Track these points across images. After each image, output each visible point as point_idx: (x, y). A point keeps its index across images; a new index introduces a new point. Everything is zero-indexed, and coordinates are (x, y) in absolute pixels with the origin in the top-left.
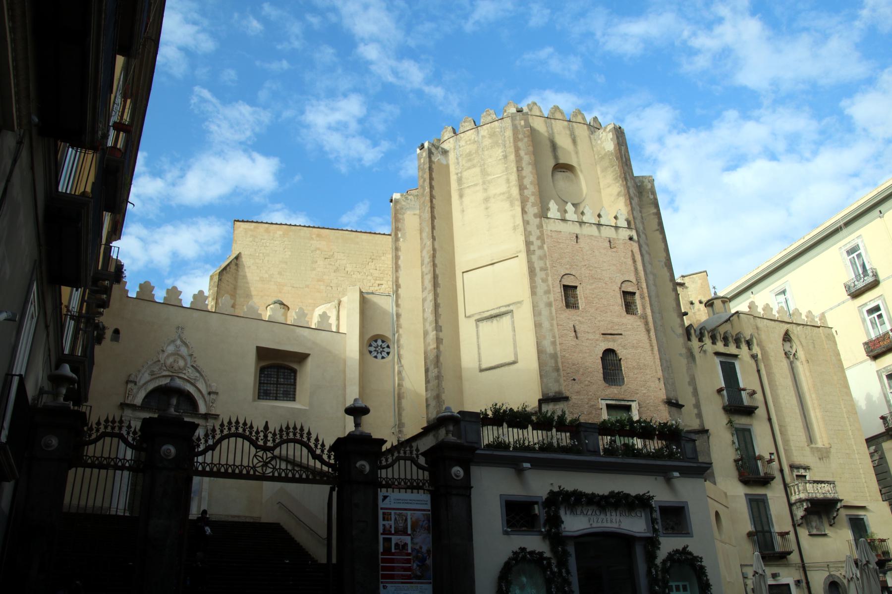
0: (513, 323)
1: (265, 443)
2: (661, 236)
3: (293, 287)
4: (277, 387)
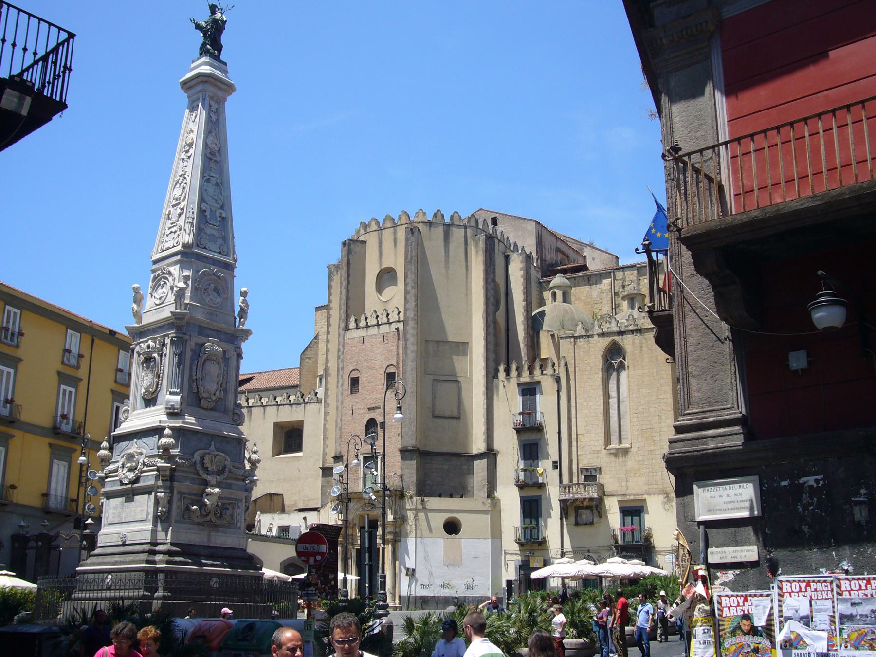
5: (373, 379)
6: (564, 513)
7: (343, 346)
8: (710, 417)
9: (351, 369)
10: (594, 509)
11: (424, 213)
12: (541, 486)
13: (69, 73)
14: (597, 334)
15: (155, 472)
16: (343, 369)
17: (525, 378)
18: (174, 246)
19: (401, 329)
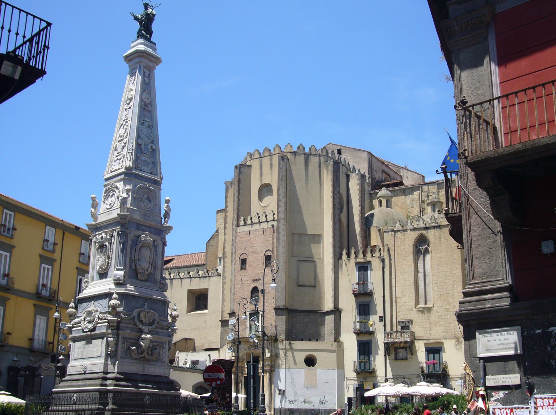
5: (256, 260)
6: (387, 352)
7: (236, 237)
8: (487, 286)
9: (241, 253)
10: (408, 349)
11: (291, 146)
12: (372, 333)
13: (48, 50)
14: (410, 229)
15: (107, 324)
16: (235, 253)
17: (361, 259)
18: (119, 169)
19: (275, 225)
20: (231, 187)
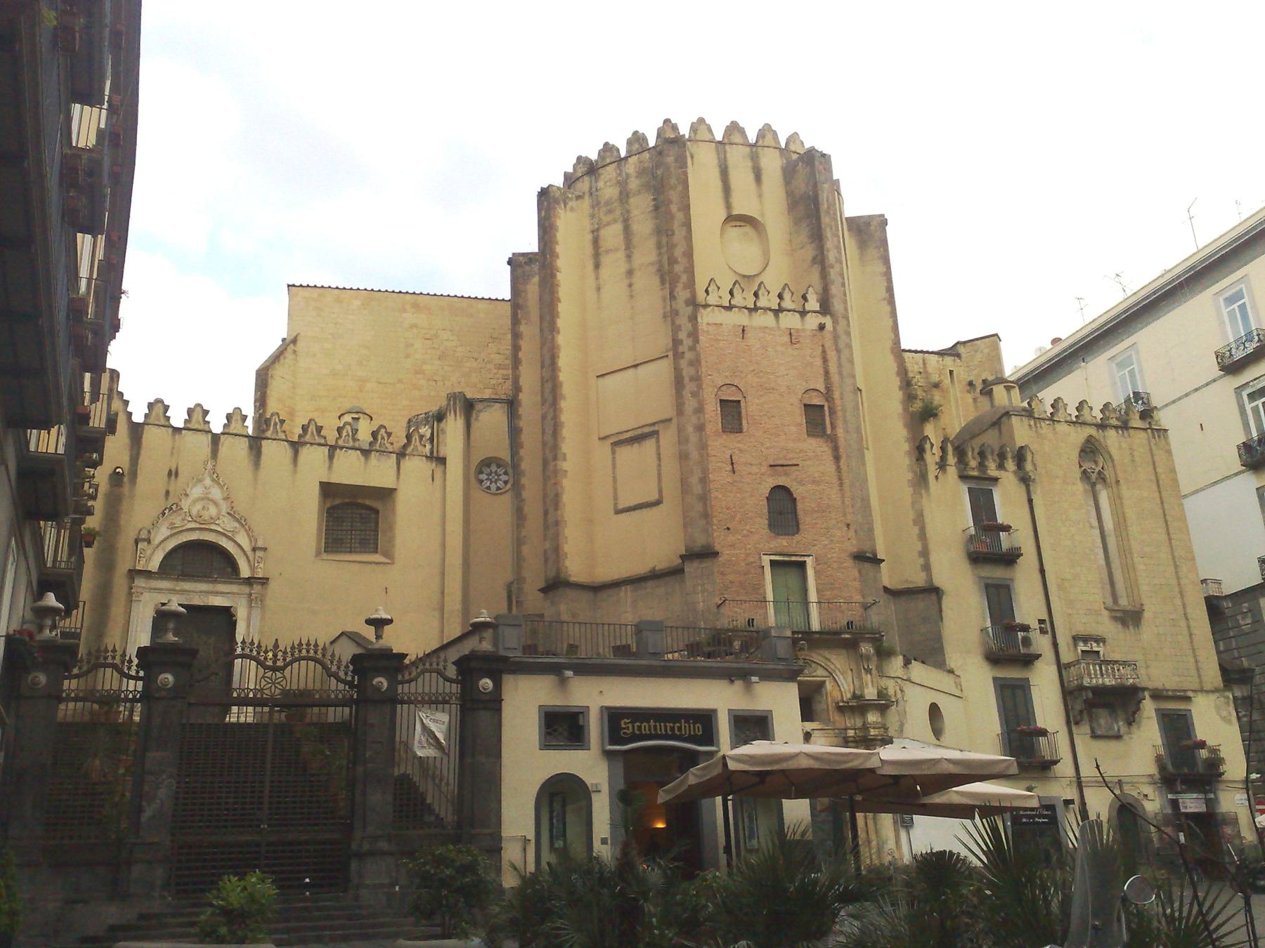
0: (658, 448)
1: (275, 662)
2: (888, 308)
3: (380, 383)
4: (351, 535)
16: (697, 379)
19: (829, 326)
20: (565, 207)
